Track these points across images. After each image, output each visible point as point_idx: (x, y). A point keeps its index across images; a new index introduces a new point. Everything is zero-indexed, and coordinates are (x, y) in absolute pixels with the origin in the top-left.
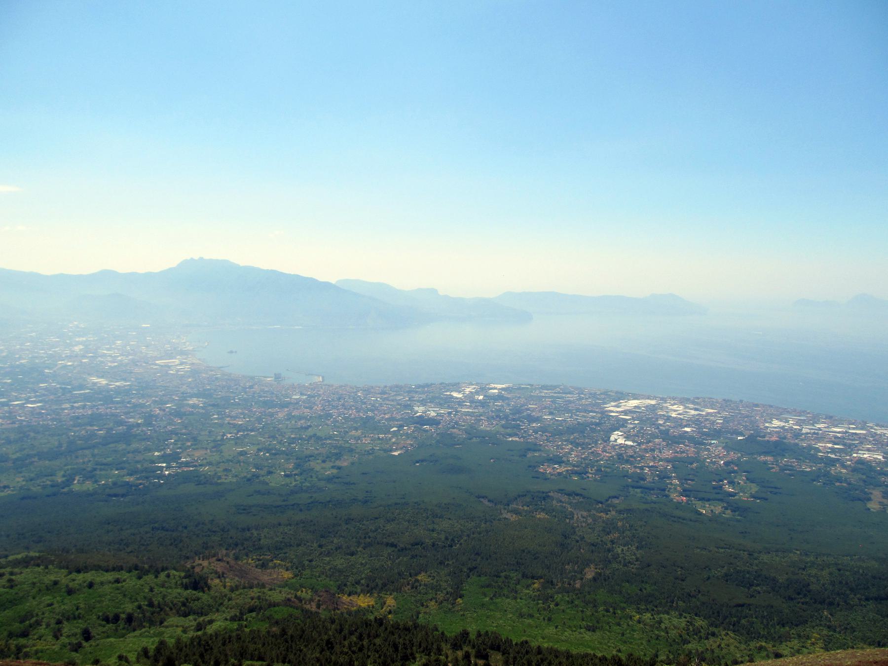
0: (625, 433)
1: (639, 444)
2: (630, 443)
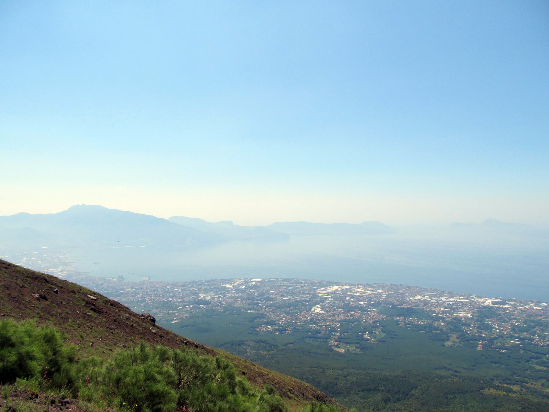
0: (322, 306)
1: (327, 312)
2: (323, 312)
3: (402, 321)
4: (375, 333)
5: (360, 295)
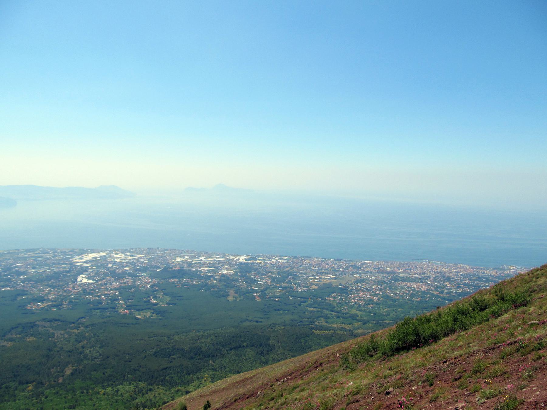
0: (87, 276)
1: (97, 281)
2: (91, 281)
4: (159, 297)
5: (121, 261)
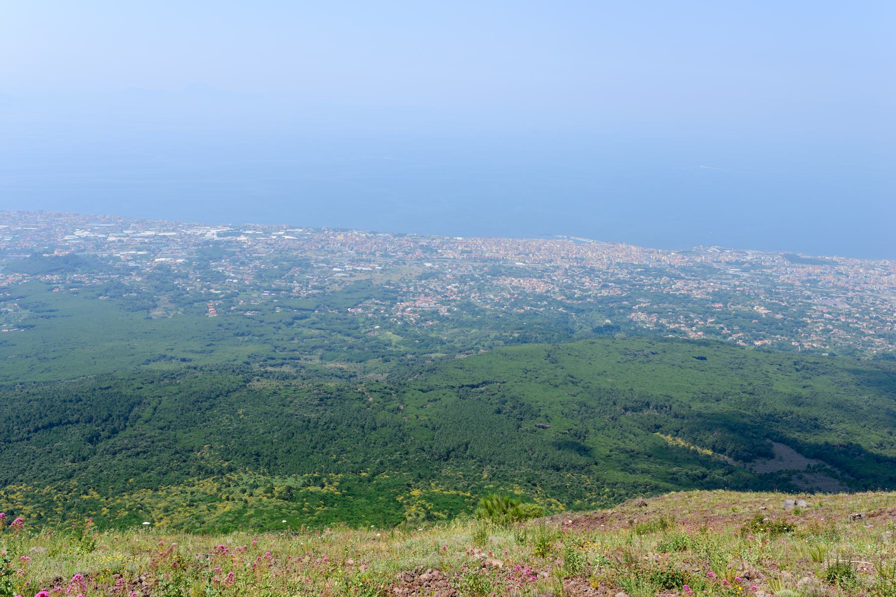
3: (59, 283)
4: (7, 312)
